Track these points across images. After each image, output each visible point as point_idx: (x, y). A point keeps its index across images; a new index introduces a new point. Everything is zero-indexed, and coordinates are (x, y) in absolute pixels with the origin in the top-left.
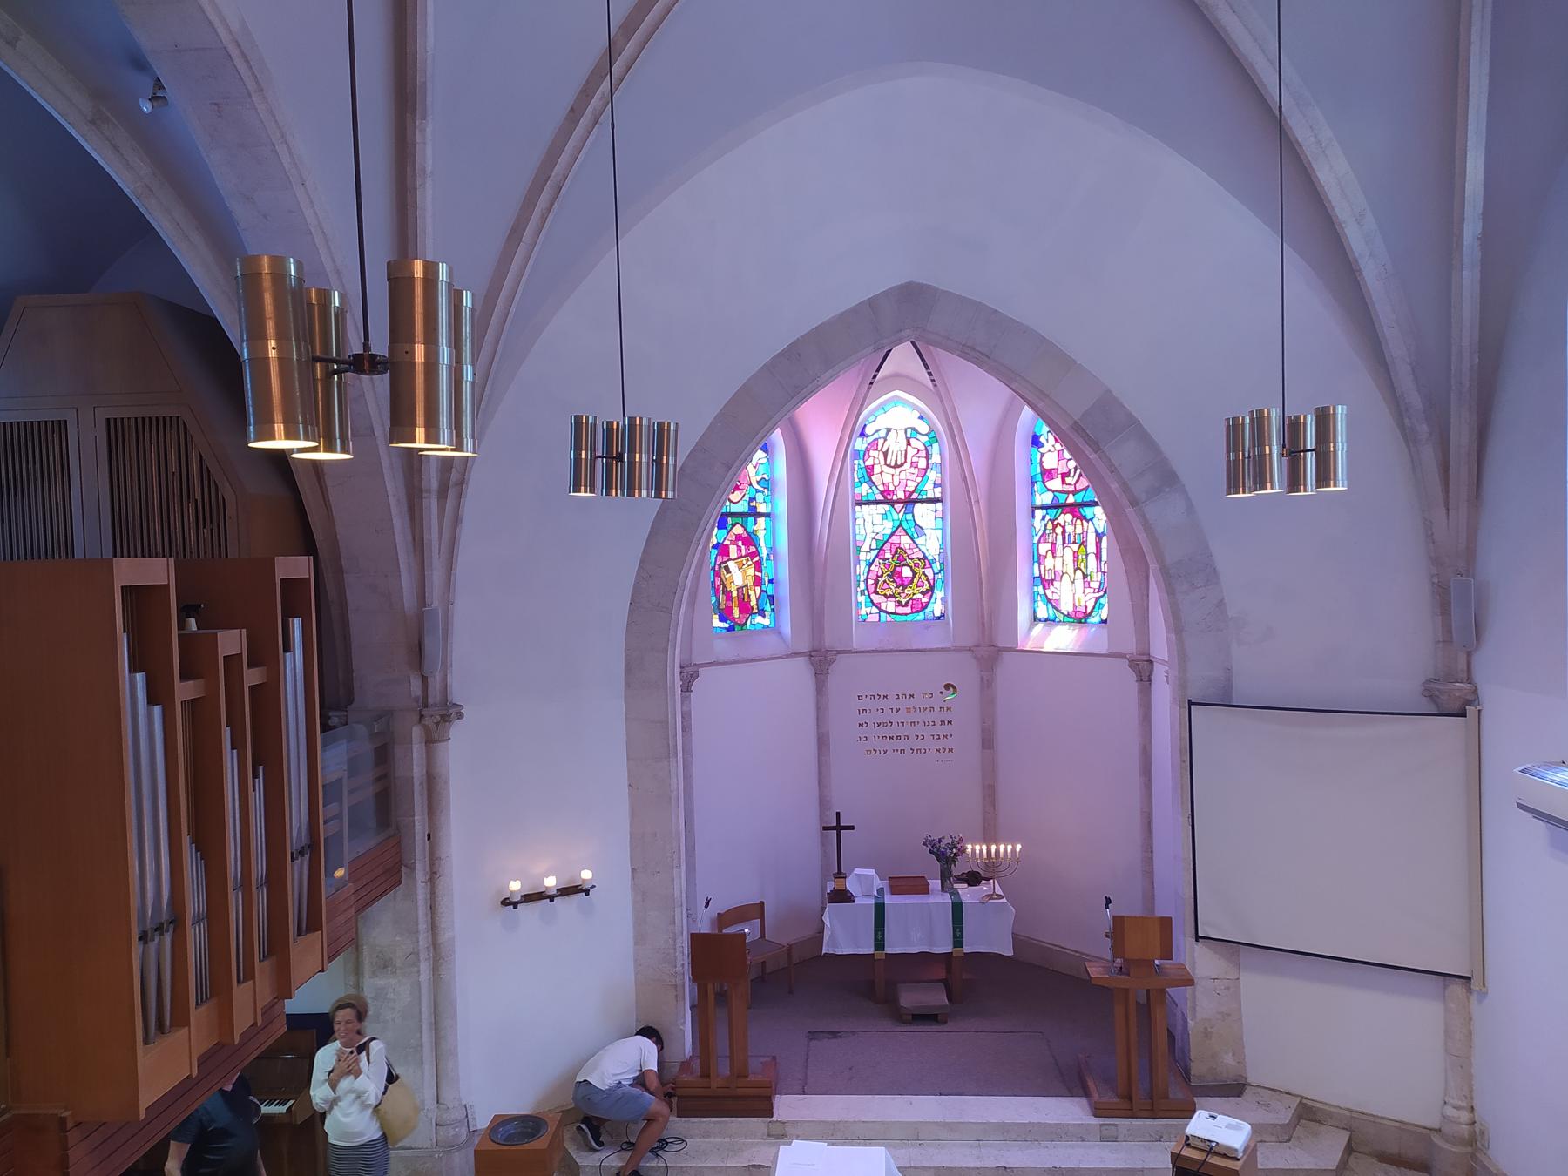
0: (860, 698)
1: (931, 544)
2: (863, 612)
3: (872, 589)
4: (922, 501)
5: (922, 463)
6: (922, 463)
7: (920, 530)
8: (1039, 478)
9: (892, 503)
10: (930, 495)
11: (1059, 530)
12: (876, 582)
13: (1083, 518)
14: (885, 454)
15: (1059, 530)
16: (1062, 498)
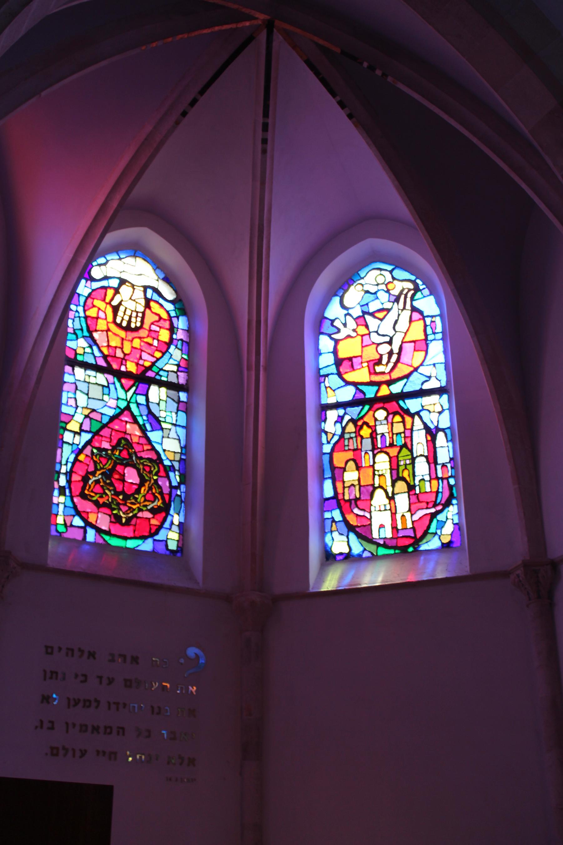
0: (49, 650)
1: (169, 445)
2: (60, 520)
3: (77, 489)
4: (161, 384)
5: (164, 336)
6: (164, 336)
7: (156, 422)
8: (333, 369)
9: (119, 375)
10: (173, 378)
11: (366, 432)
12: (85, 479)
13: (407, 412)
14: (115, 310)
15: (366, 432)
16: (370, 392)
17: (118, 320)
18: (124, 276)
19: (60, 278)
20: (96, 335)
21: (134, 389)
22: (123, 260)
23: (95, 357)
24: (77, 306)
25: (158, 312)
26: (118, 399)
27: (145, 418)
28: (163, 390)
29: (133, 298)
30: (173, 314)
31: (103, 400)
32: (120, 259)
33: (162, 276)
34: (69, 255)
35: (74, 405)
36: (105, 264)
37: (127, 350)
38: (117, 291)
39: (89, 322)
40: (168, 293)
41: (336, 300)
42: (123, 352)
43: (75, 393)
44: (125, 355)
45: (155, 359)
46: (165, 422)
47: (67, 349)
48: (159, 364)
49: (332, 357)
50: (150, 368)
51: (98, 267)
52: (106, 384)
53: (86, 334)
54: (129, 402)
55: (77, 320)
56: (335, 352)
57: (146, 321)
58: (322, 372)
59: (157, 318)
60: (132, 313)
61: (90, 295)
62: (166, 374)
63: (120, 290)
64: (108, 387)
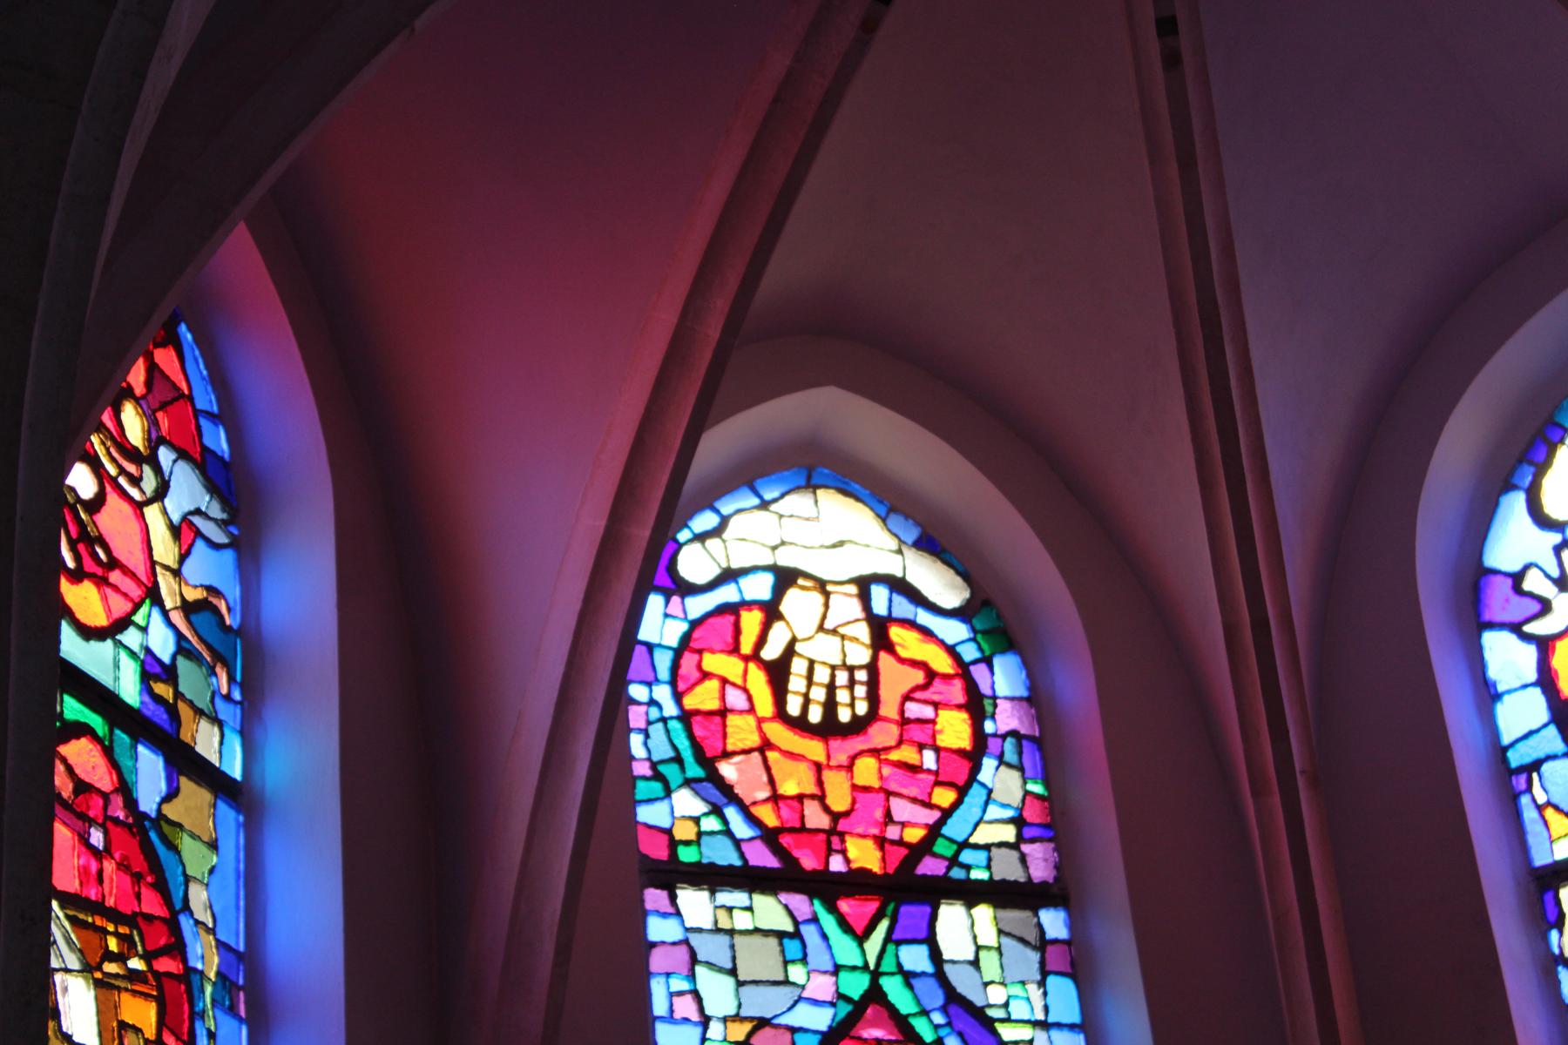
4: (971, 894)
5: (954, 730)
6: (954, 730)
10: (1007, 868)
14: (778, 673)
17: (794, 707)
18: (786, 559)
19: (578, 606)
20: (727, 770)
21: (884, 925)
22: (773, 507)
23: (737, 843)
24: (649, 684)
25: (919, 657)
26: (837, 969)
27: (938, 1018)
28: (984, 912)
29: (828, 625)
30: (969, 653)
31: (786, 982)
32: (764, 505)
33: (912, 534)
34: (592, 523)
35: (695, 1017)
36: (717, 532)
37: (839, 800)
38: (771, 612)
39: (698, 732)
40: (941, 585)
41: (1515, 504)
42: (827, 809)
43: (692, 976)
44: (836, 817)
45: (937, 814)
46: (1008, 1020)
47: (642, 834)
48: (955, 828)
49: (1537, 698)
50: (924, 847)
51: (697, 546)
52: (789, 928)
53: (694, 771)
54: (876, 975)
55: (657, 730)
56: (1546, 679)
57: (884, 692)
58: (1516, 758)
59: (919, 677)
60: (833, 677)
61: (686, 639)
62: (981, 856)
63: (783, 608)
64: (797, 935)
